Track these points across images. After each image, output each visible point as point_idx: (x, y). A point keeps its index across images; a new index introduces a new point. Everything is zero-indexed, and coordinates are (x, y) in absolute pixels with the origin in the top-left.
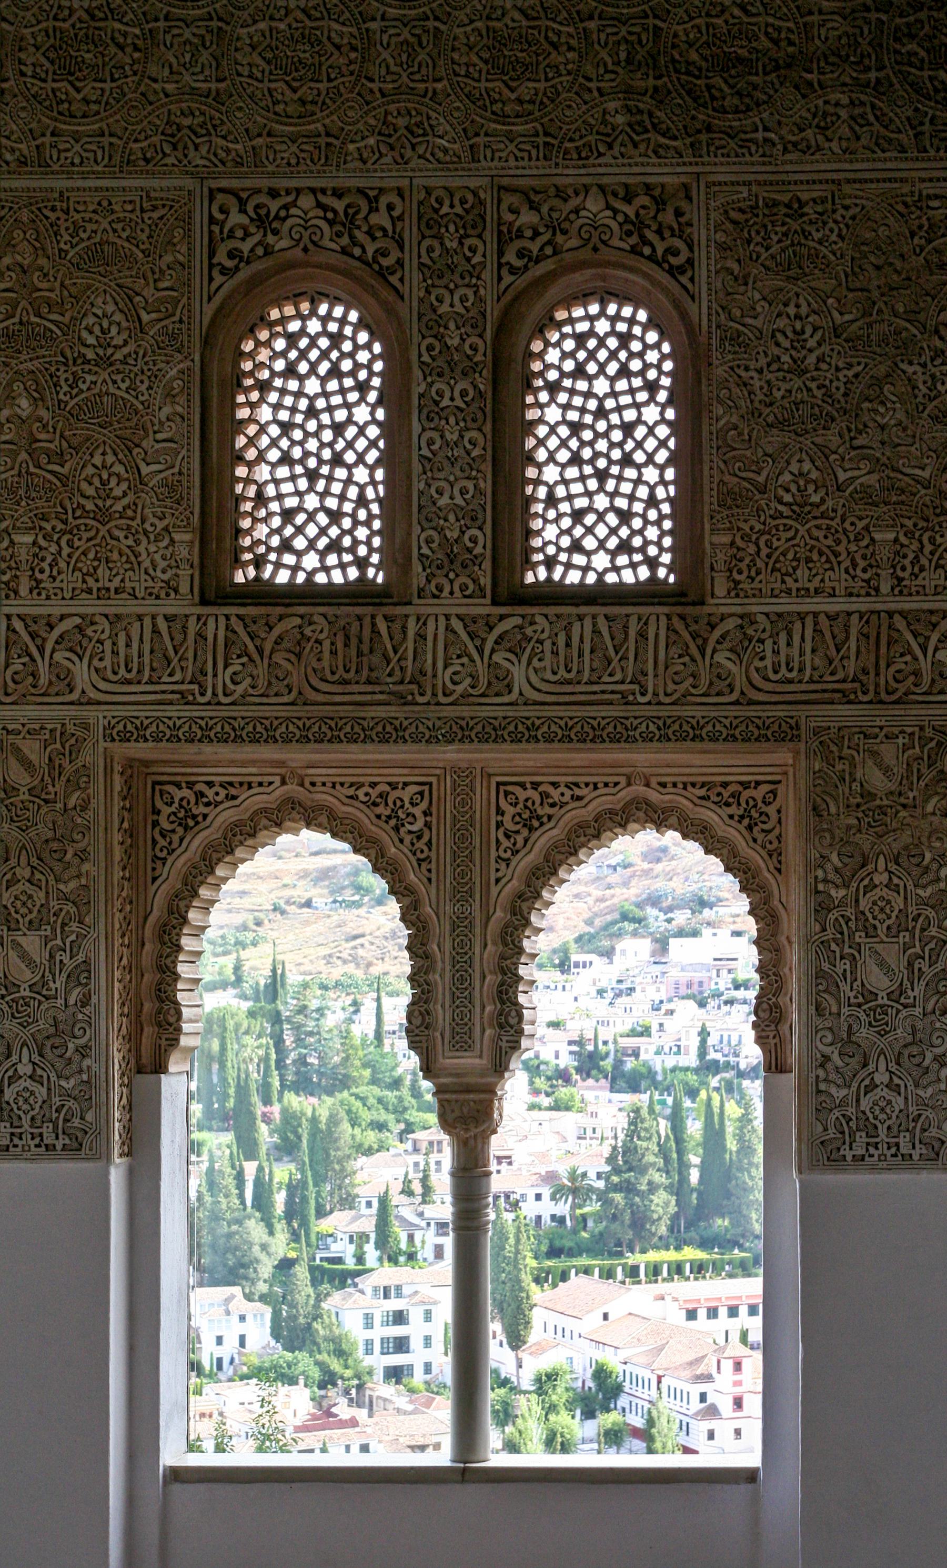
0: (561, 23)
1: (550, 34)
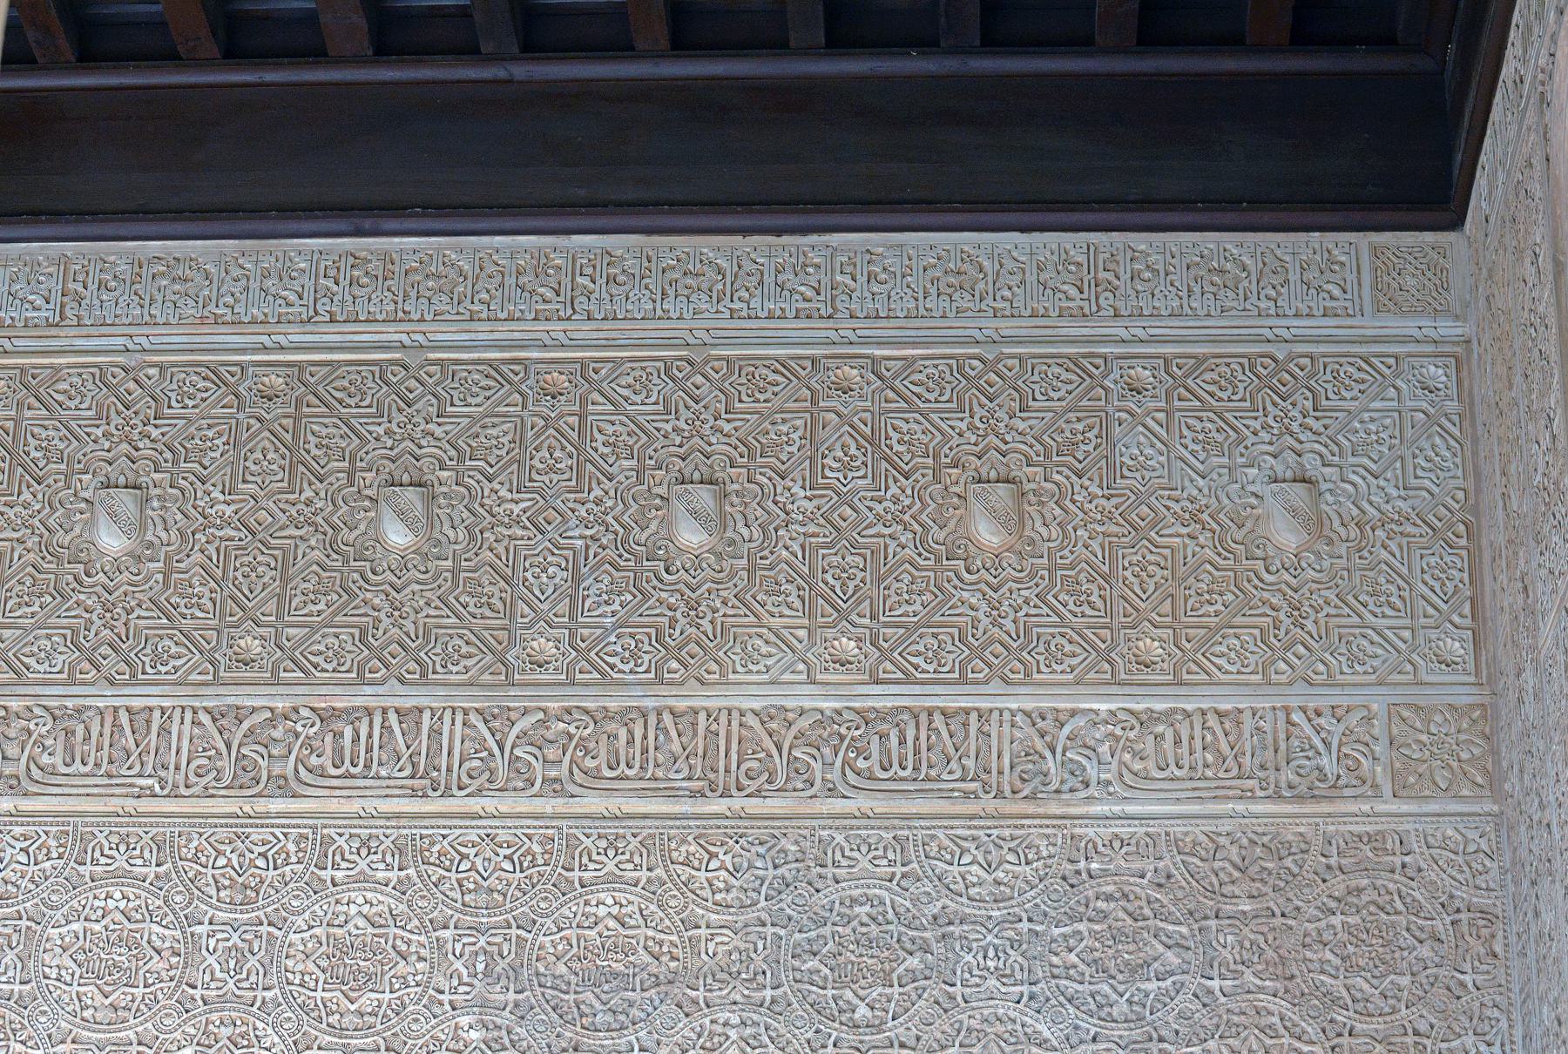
0: (411, 932)
1: (399, 942)
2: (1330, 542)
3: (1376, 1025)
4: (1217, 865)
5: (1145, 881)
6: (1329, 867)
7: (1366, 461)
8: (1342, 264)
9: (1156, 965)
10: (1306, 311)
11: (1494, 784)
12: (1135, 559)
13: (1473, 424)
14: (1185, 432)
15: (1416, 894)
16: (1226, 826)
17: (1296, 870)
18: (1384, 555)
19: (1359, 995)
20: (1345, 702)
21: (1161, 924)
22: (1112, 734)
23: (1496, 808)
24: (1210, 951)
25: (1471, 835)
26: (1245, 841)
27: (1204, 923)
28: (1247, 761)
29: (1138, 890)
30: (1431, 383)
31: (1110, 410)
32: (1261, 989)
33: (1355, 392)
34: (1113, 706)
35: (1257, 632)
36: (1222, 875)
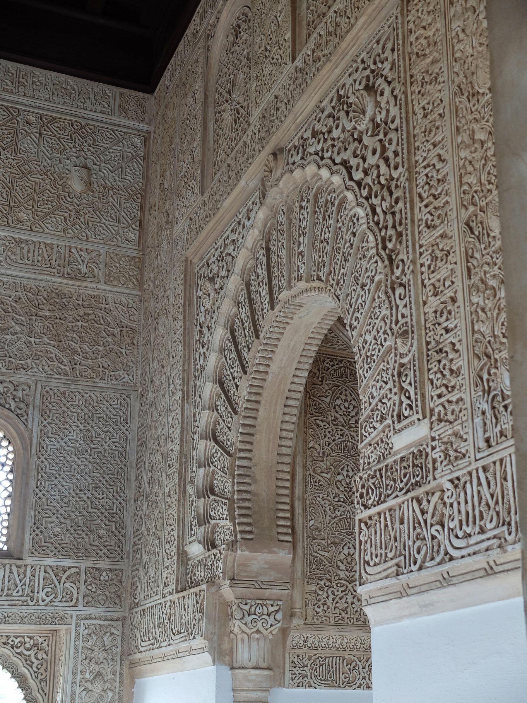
2: (93, 192)
3: (89, 362)
4: (38, 297)
5: (11, 299)
6: (79, 304)
7: (109, 166)
8: (109, 96)
9: (11, 330)
10: (94, 110)
11: (140, 285)
12: (21, 183)
13: (148, 162)
14: (45, 142)
15: (109, 319)
16: (43, 284)
17: (67, 304)
18: (111, 199)
19: (84, 351)
20: (91, 248)
21: (15, 315)
22: (5, 244)
23: (140, 294)
24: (32, 327)
25: (130, 301)
26: (49, 291)
27: (31, 317)
28: (53, 262)
29: (8, 302)
30: (135, 144)
31: (18, 129)
32: (49, 344)
33: (108, 142)
34: (7, 234)
35: (63, 218)
36: (39, 301)
